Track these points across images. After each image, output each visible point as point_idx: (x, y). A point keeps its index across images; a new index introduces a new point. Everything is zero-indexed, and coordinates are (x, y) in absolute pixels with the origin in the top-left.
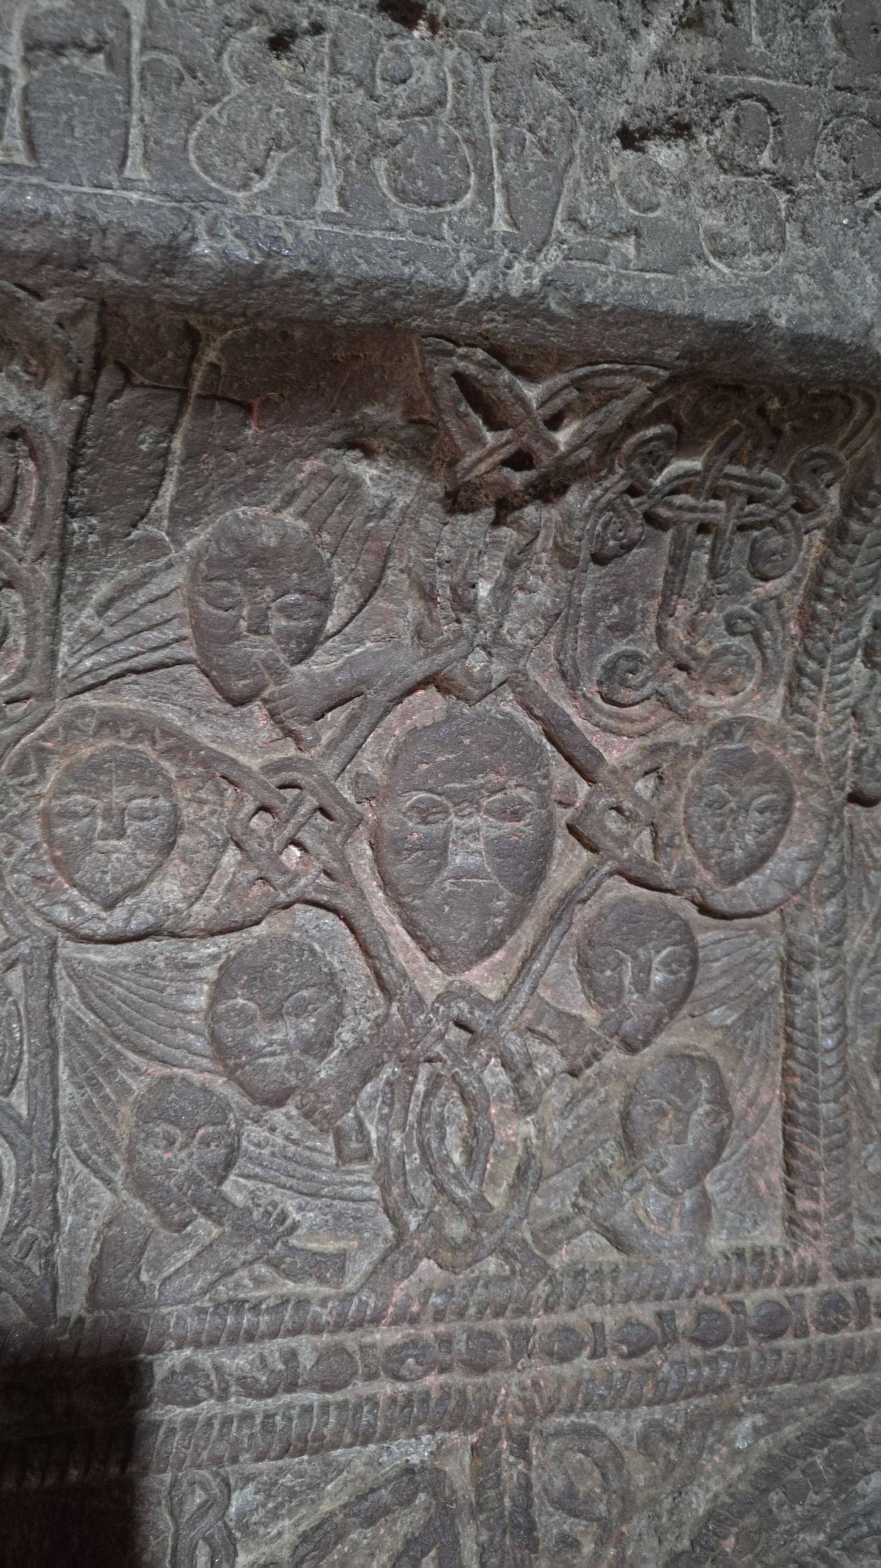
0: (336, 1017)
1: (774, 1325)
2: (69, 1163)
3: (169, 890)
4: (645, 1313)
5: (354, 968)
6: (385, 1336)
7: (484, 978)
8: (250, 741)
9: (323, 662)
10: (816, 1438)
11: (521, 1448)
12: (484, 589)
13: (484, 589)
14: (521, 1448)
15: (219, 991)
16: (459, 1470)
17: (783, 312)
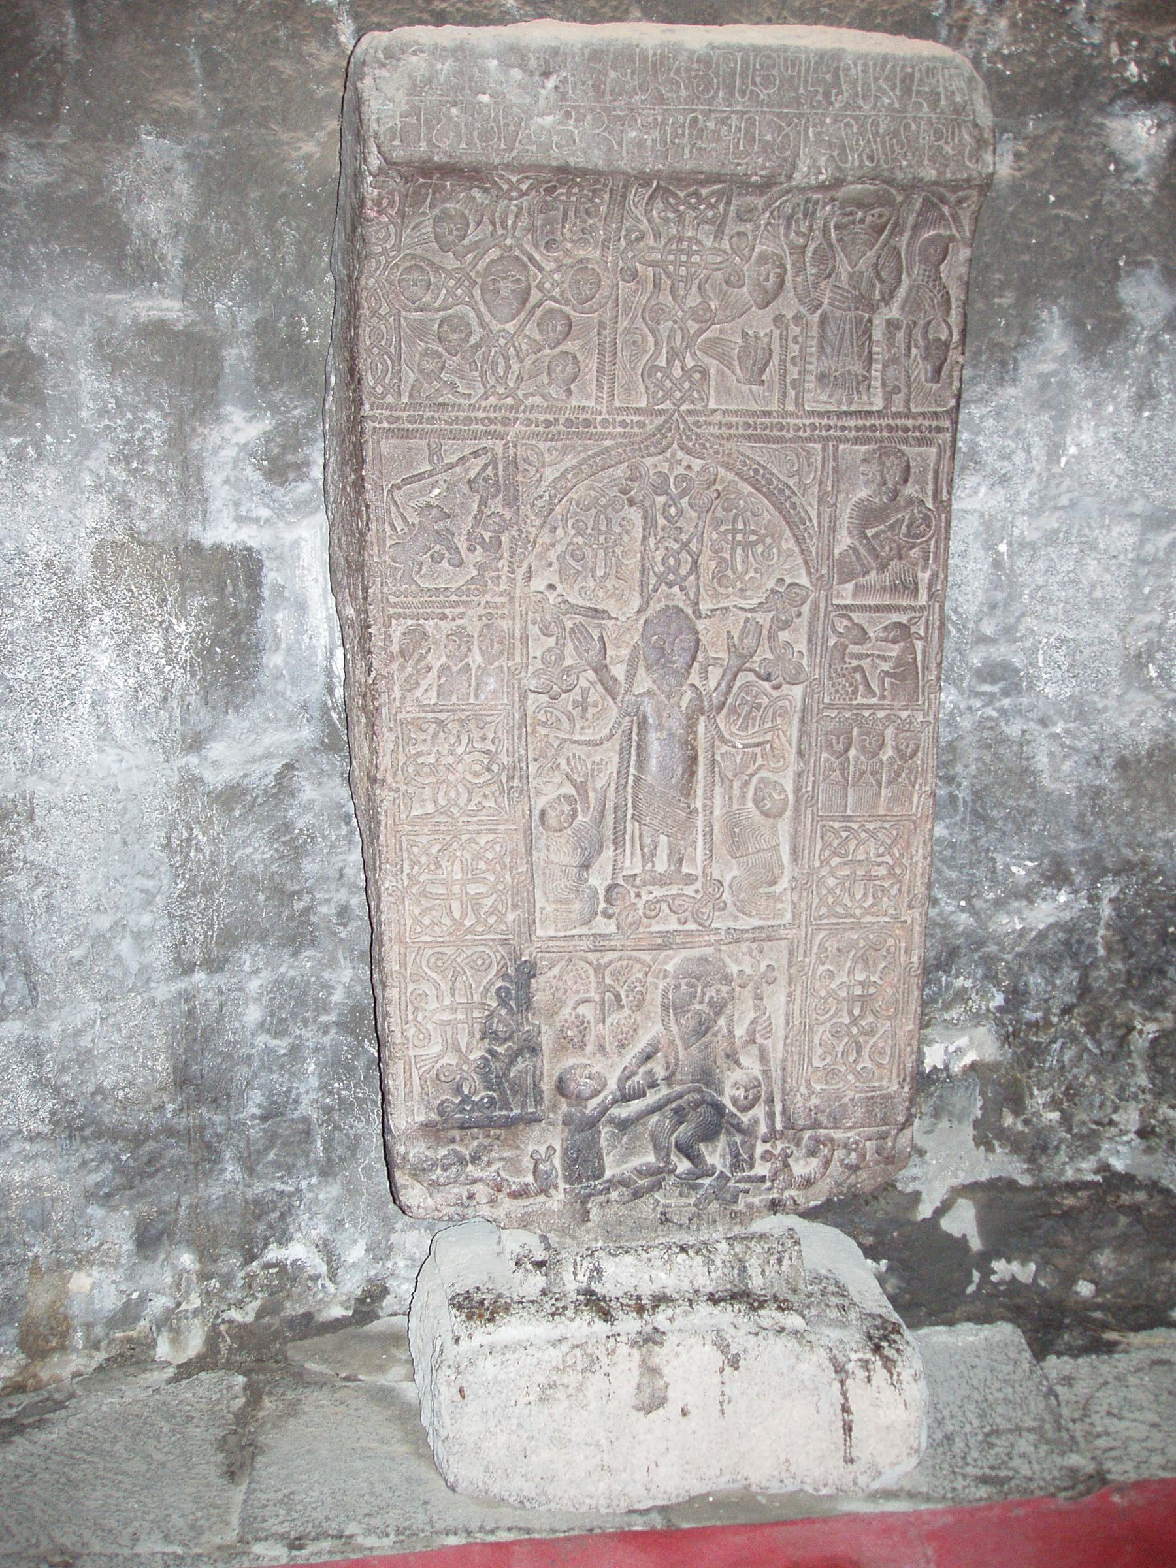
0: (469, 334)
1: (587, 423)
2: (404, 367)
3: (427, 299)
4: (551, 417)
5: (475, 322)
6: (481, 415)
7: (510, 327)
8: (450, 262)
9: (466, 242)
10: (597, 454)
11: (515, 446)
12: (510, 222)
13: (510, 222)
14: (515, 446)
15: (440, 326)
16: (499, 450)
17: (572, 161)
